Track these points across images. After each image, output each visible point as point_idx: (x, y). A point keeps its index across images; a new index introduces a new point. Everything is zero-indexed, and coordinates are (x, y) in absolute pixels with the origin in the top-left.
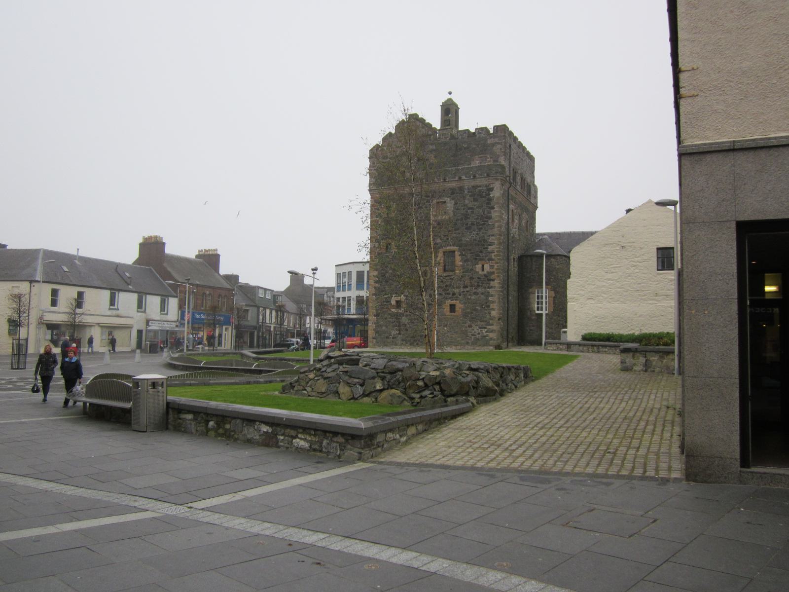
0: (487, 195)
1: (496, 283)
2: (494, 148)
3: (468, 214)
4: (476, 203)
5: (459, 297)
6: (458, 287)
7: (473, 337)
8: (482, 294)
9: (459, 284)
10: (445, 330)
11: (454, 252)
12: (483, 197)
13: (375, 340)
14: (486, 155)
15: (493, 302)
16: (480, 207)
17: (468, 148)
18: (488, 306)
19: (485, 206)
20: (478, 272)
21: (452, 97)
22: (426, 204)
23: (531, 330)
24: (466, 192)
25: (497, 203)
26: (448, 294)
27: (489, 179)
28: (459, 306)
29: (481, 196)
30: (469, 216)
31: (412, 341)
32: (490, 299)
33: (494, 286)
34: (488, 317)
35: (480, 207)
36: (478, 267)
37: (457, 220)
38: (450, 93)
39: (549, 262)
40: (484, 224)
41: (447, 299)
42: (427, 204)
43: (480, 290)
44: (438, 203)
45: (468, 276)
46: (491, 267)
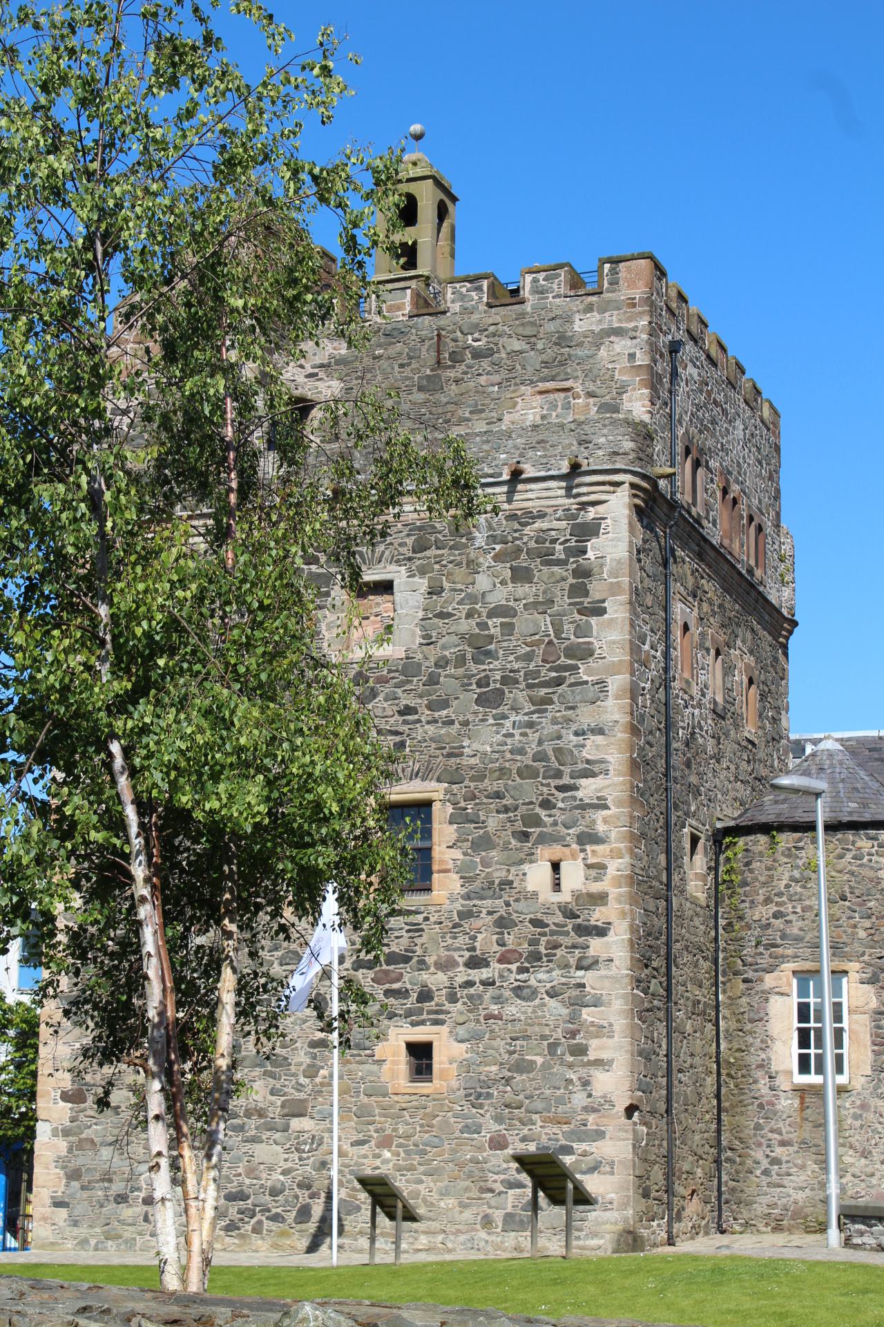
0: (570, 552)
1: (615, 947)
2: (603, 352)
3: (491, 637)
4: (524, 590)
5: (447, 1006)
6: (445, 965)
7: (511, 1192)
8: (552, 994)
9: (448, 948)
10: (386, 1161)
11: (427, 805)
12: (559, 563)
13: (63, 1213)
15: (601, 1031)
16: (542, 605)
17: (488, 353)
18: (581, 1050)
19: (563, 602)
20: (535, 895)
23: (775, 1161)
25: (615, 589)
26: (402, 994)
28: (448, 1052)
29: (547, 558)
30: (492, 647)
32: (587, 1014)
33: (604, 956)
34: (579, 1099)
35: (542, 605)
36: (537, 876)
37: (442, 663)
39: (849, 856)
40: (559, 682)
41: (392, 1016)
43: (540, 978)
45: (490, 913)
46: (597, 869)
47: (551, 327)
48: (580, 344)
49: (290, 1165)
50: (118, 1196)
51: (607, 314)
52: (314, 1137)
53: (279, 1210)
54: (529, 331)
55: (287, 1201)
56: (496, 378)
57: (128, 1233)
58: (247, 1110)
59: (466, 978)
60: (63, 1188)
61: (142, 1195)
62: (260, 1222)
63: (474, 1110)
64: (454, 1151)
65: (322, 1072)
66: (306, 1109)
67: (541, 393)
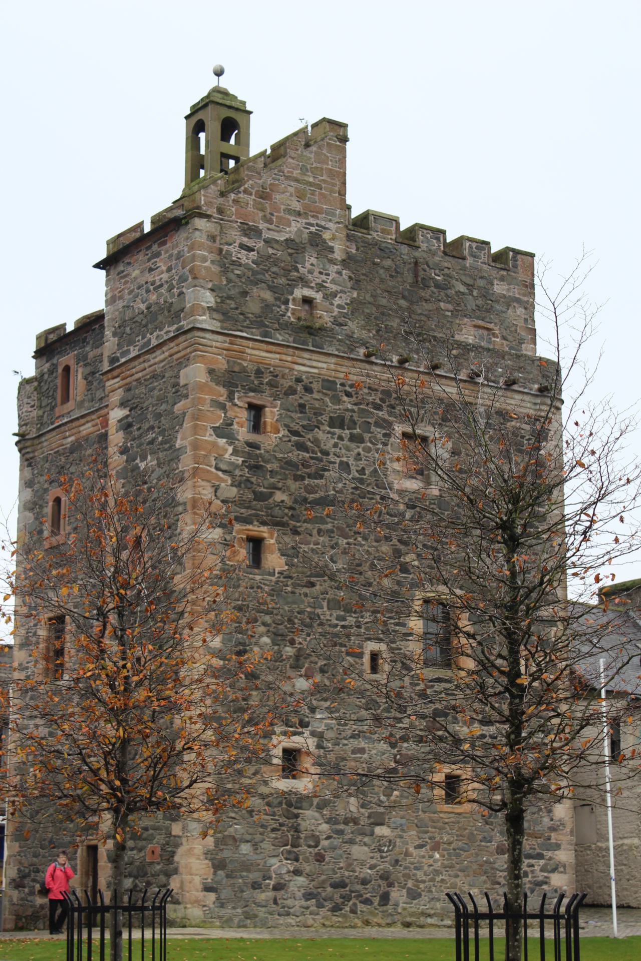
10: (436, 861)
13: (212, 896)
14: (491, 326)
21: (225, 83)
22: (373, 428)
24: (482, 422)
27: (542, 404)
31: (337, 897)
38: (219, 73)
42: (379, 432)
44: (405, 435)
47: (481, 283)
48: (497, 301)
49: (374, 861)
50: (255, 883)
51: (512, 286)
52: (390, 841)
53: (368, 895)
54: (468, 281)
55: (373, 889)
56: (450, 307)
57: (262, 912)
58: (346, 818)
59: (481, 732)
60: (211, 876)
61: (272, 883)
62: (355, 904)
63: (488, 826)
64: (477, 855)
65: (395, 793)
66: (384, 819)
67: (475, 326)
